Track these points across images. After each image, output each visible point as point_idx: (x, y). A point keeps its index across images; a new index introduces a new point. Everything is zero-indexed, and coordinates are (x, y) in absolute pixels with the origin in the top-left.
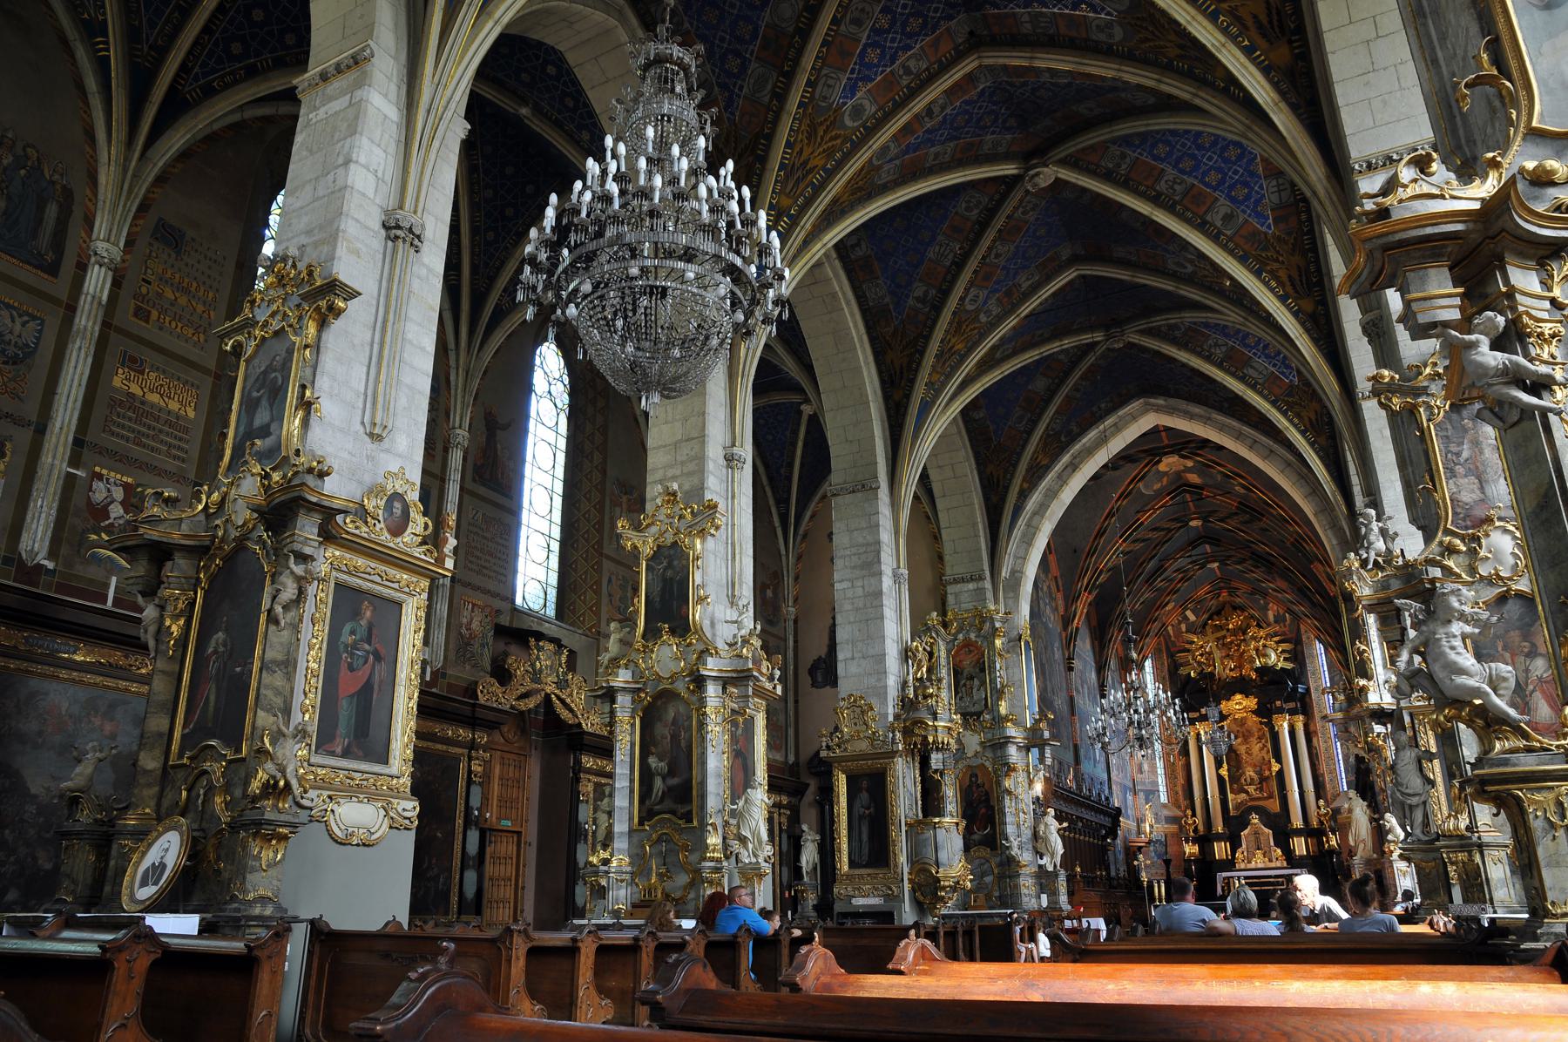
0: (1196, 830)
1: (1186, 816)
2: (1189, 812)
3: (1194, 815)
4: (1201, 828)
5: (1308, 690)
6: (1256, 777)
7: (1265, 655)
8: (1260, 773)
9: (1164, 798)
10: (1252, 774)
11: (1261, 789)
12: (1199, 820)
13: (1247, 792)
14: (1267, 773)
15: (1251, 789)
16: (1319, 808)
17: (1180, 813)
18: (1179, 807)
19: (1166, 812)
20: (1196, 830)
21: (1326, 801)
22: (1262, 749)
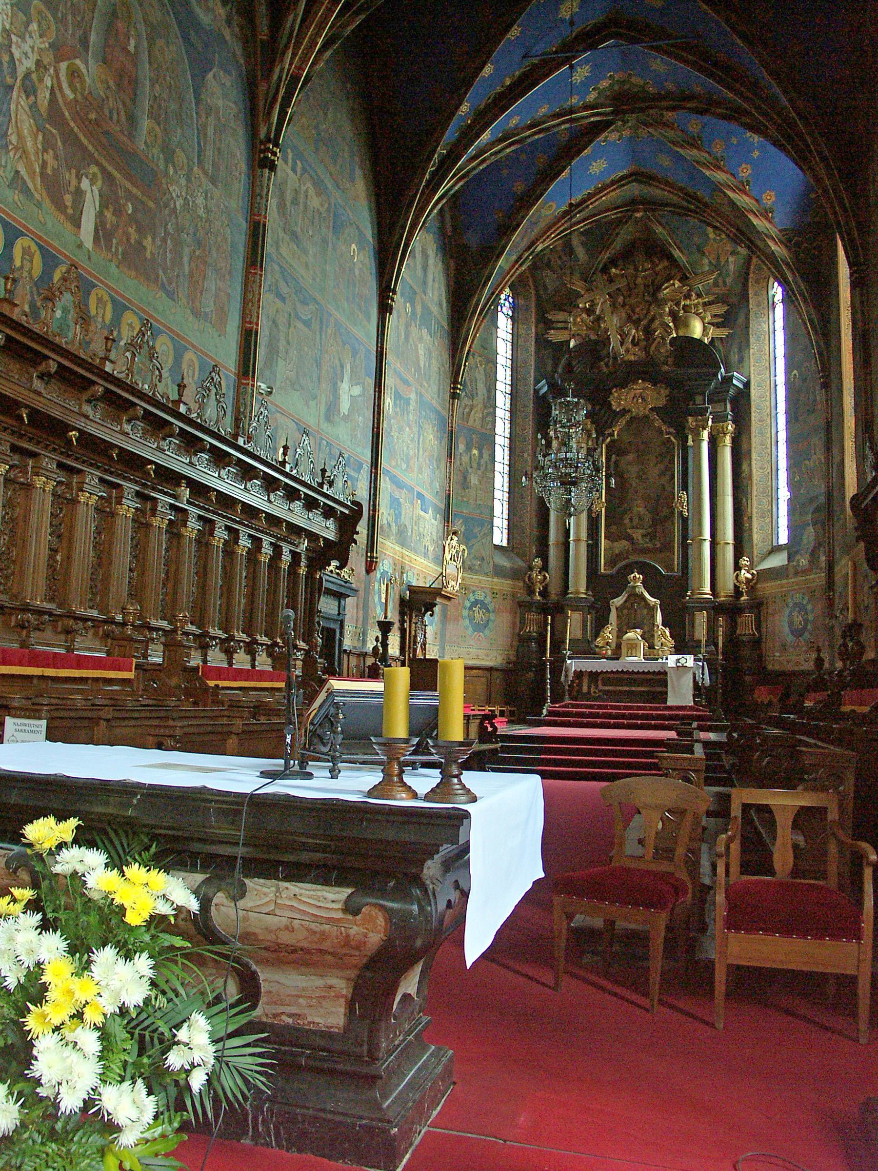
0: (544, 593)
1: (531, 568)
2: (538, 562)
3: (545, 568)
4: (554, 590)
5: (747, 385)
6: (648, 517)
7: (687, 325)
8: (655, 512)
9: (500, 537)
10: (641, 510)
11: (652, 536)
12: (553, 576)
13: (630, 539)
14: (665, 512)
15: (637, 534)
16: (737, 567)
17: (521, 563)
18: (522, 556)
19: (504, 562)
20: (544, 593)
21: (751, 561)
22: (662, 474)
